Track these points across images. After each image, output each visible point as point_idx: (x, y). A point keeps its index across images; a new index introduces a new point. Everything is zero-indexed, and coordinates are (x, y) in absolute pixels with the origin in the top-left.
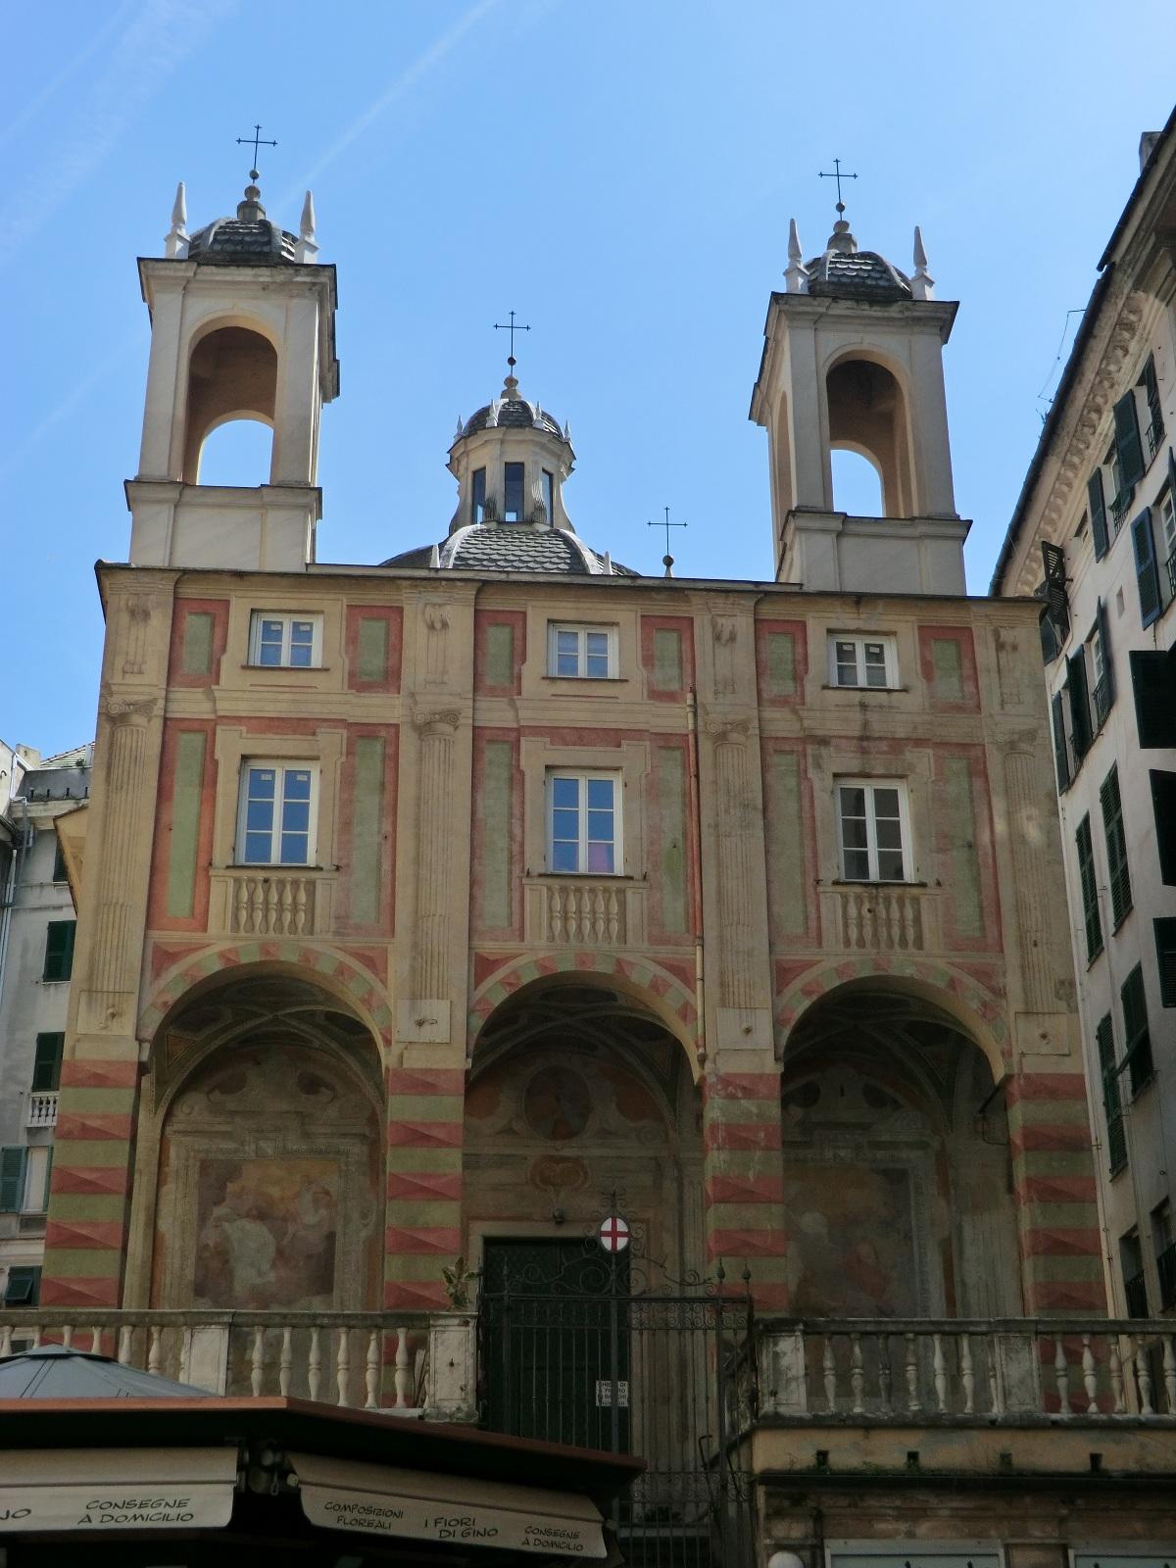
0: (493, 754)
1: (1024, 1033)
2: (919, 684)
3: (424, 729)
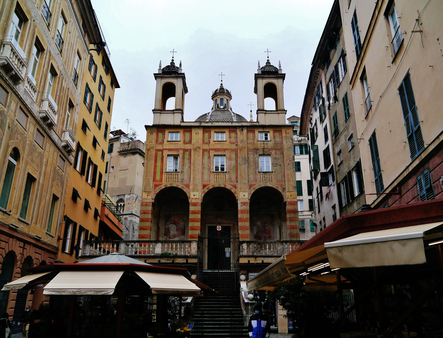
0: (206, 153)
1: (288, 194)
2: (273, 140)
3: (195, 150)
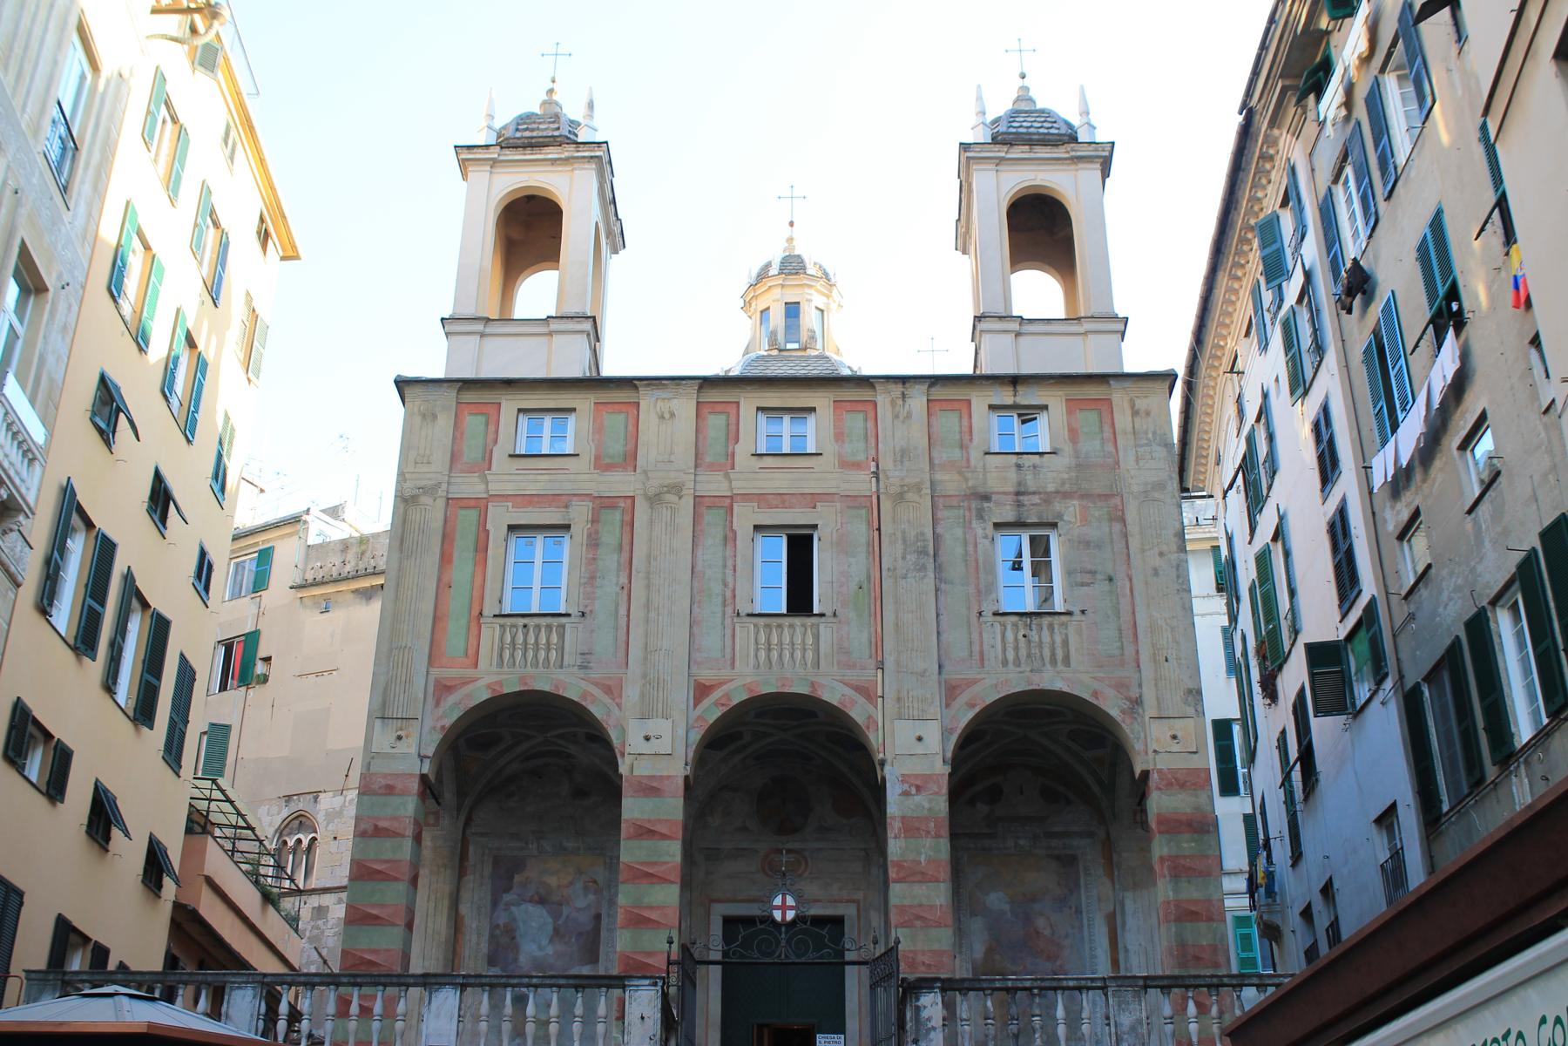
0: (712, 518)
1: (1158, 734)
2: (1067, 448)
3: (655, 500)
